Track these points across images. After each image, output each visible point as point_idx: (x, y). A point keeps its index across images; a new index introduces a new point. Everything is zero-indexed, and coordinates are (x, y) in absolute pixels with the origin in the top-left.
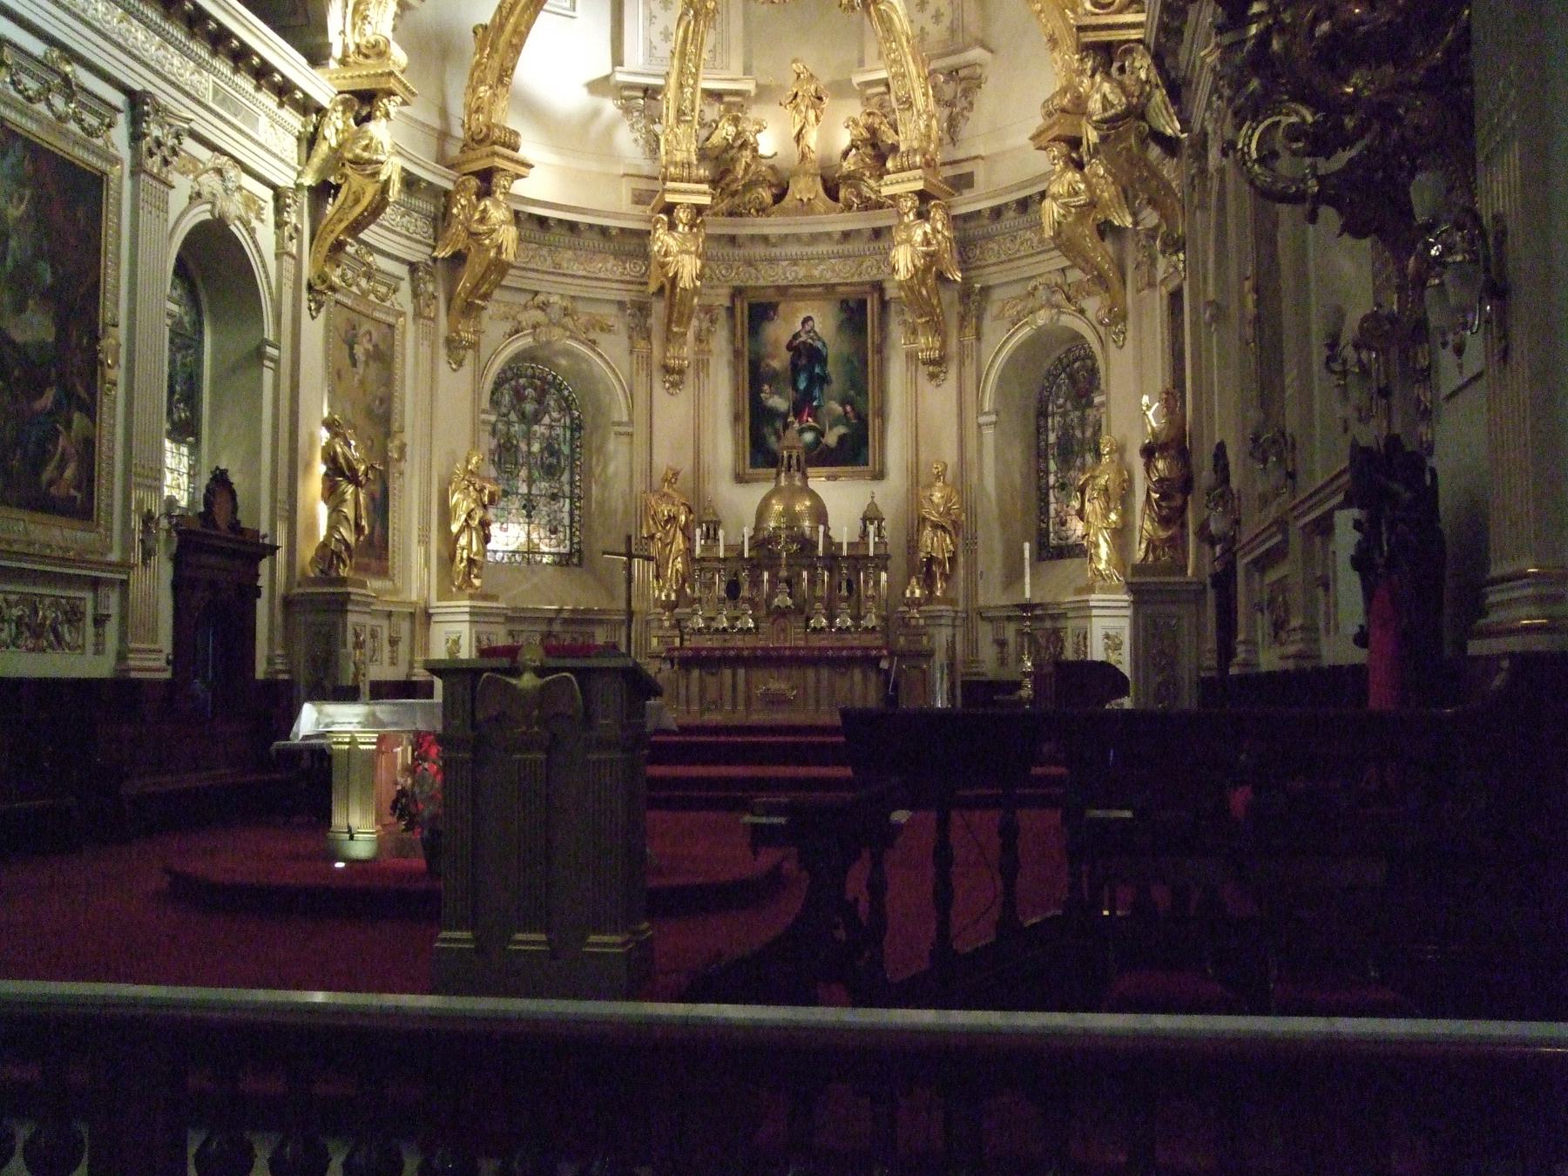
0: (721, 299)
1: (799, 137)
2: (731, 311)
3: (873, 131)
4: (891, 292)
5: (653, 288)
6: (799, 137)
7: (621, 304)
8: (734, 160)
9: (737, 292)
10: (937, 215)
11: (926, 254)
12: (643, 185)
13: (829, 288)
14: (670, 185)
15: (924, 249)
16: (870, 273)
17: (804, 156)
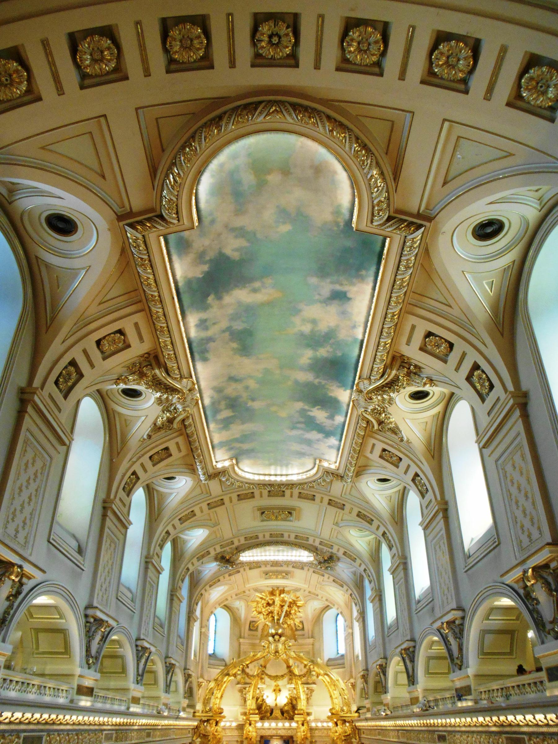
0: (258, 739)
1: (276, 700)
2: (260, 741)
3: (291, 700)
4: (295, 739)
5: (244, 737)
6: (276, 700)
7: (237, 741)
8: (262, 705)
9: (262, 737)
10: (305, 724)
11: (304, 735)
12: (243, 711)
13: (282, 737)
14: (251, 716)
15: (303, 734)
16: (290, 733)
17: (276, 705)
